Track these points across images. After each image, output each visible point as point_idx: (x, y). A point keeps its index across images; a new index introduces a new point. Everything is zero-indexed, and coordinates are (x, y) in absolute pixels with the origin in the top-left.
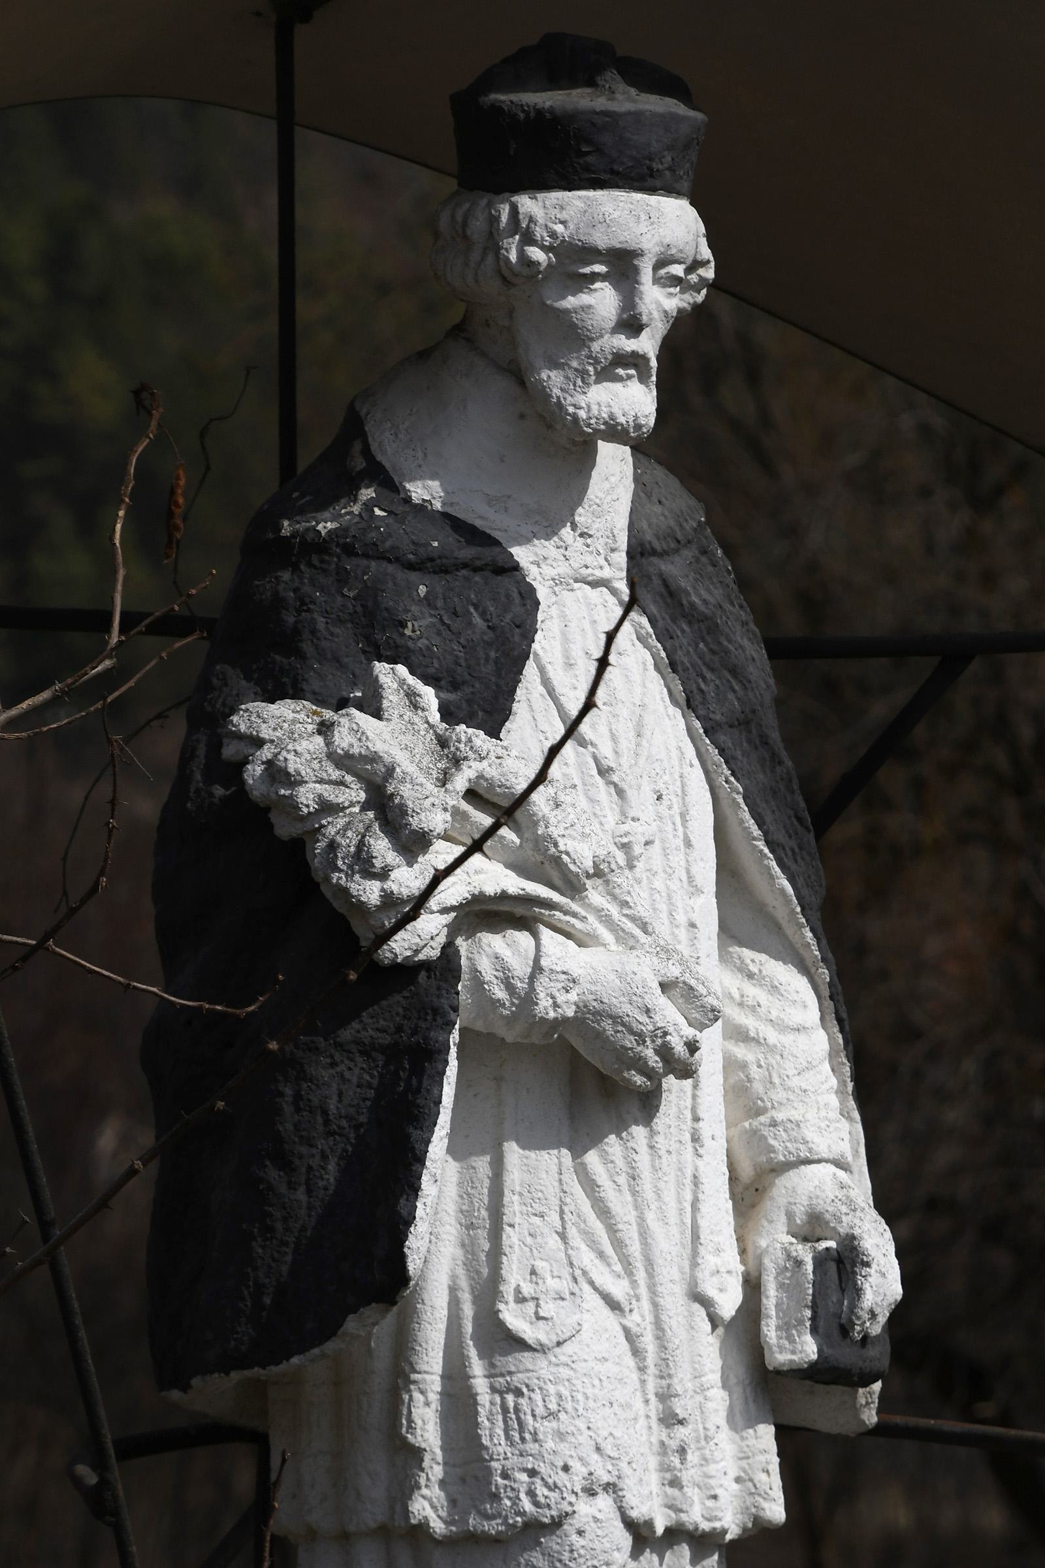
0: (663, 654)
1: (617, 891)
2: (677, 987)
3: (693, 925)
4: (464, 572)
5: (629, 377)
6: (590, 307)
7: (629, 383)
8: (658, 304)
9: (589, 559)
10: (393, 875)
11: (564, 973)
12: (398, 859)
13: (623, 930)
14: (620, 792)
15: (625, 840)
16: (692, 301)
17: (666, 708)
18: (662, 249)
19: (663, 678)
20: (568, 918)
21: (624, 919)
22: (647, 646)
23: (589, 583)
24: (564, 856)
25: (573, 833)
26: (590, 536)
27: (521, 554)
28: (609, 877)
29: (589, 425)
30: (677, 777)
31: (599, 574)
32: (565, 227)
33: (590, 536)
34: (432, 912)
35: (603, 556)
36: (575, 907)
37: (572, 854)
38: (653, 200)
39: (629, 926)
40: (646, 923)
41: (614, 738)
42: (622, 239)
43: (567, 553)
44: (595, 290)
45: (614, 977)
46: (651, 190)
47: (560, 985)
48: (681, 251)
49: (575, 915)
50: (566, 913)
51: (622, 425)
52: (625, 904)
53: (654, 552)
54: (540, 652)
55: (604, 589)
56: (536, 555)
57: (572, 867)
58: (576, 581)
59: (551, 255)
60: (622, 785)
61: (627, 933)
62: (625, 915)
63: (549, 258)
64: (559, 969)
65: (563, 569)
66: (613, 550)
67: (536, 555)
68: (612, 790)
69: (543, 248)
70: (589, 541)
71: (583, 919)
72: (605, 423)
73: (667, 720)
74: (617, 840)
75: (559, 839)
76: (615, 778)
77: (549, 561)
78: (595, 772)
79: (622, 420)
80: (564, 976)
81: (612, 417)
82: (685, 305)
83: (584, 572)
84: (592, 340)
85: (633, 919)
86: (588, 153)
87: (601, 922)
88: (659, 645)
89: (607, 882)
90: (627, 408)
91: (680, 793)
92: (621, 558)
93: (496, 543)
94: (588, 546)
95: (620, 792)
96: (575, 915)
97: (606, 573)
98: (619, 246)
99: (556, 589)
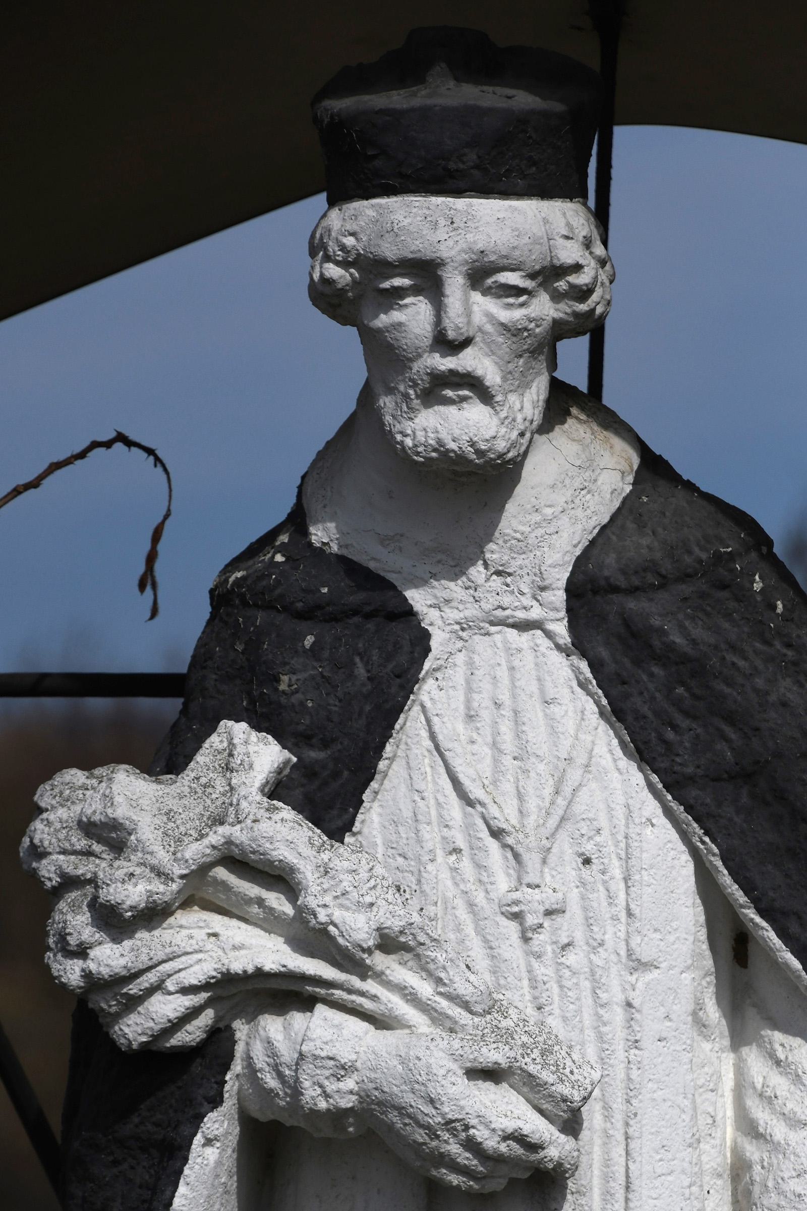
0: (604, 701)
1: (431, 966)
2: (514, 1074)
3: (629, 1005)
4: (356, 619)
5: (464, 399)
6: (400, 324)
7: (465, 405)
8: (491, 317)
9: (507, 600)
10: (92, 953)
12: (97, 935)
13: (436, 1011)
14: (517, 856)
15: (515, 909)
16: (569, 310)
17: (615, 761)
18: (474, 257)
19: (612, 727)
20: (353, 997)
21: (438, 998)
22: (590, 694)
23: (513, 626)
24: (331, 928)
25: (347, 903)
26: (510, 574)
27: (417, 598)
28: (420, 950)
29: (418, 454)
30: (620, 837)
31: (521, 615)
32: (357, 239)
33: (510, 574)
34: (170, 993)
35: (529, 595)
36: (370, 986)
37: (340, 925)
38: (460, 203)
41: (520, 797)
42: (413, 248)
43: (476, 594)
44: (406, 306)
45: (396, 1062)
46: (458, 193)
47: (327, 1073)
48: (506, 257)
49: (362, 994)
50: (350, 991)
51: (453, 451)
52: (439, 981)
53: (615, 589)
54: (428, 704)
55: (539, 632)
56: (436, 597)
57: (341, 941)
58: (492, 623)
59: (352, 270)
60: (520, 849)
61: (441, 1014)
62: (440, 994)
63: (351, 275)
64: (323, 1054)
65: (471, 611)
66: (543, 589)
67: (436, 597)
68: (509, 855)
69: (338, 263)
70: (509, 580)
71: (374, 998)
72: (435, 450)
73: (617, 774)
74: (504, 909)
75: (318, 910)
76: (510, 841)
77: (454, 604)
78: (485, 834)
79: (453, 446)
80: (332, 1063)
81: (440, 442)
82: (561, 315)
83: (499, 613)
84: (411, 360)
85: (452, 998)
86: (374, 157)
87: (407, 1001)
88: (600, 692)
89: (418, 956)
90: (457, 432)
91: (623, 856)
92: (559, 597)
93: (392, 587)
94: (508, 585)
95: (517, 856)
96: (362, 994)
97: (536, 613)
98: (411, 256)
99: (464, 634)
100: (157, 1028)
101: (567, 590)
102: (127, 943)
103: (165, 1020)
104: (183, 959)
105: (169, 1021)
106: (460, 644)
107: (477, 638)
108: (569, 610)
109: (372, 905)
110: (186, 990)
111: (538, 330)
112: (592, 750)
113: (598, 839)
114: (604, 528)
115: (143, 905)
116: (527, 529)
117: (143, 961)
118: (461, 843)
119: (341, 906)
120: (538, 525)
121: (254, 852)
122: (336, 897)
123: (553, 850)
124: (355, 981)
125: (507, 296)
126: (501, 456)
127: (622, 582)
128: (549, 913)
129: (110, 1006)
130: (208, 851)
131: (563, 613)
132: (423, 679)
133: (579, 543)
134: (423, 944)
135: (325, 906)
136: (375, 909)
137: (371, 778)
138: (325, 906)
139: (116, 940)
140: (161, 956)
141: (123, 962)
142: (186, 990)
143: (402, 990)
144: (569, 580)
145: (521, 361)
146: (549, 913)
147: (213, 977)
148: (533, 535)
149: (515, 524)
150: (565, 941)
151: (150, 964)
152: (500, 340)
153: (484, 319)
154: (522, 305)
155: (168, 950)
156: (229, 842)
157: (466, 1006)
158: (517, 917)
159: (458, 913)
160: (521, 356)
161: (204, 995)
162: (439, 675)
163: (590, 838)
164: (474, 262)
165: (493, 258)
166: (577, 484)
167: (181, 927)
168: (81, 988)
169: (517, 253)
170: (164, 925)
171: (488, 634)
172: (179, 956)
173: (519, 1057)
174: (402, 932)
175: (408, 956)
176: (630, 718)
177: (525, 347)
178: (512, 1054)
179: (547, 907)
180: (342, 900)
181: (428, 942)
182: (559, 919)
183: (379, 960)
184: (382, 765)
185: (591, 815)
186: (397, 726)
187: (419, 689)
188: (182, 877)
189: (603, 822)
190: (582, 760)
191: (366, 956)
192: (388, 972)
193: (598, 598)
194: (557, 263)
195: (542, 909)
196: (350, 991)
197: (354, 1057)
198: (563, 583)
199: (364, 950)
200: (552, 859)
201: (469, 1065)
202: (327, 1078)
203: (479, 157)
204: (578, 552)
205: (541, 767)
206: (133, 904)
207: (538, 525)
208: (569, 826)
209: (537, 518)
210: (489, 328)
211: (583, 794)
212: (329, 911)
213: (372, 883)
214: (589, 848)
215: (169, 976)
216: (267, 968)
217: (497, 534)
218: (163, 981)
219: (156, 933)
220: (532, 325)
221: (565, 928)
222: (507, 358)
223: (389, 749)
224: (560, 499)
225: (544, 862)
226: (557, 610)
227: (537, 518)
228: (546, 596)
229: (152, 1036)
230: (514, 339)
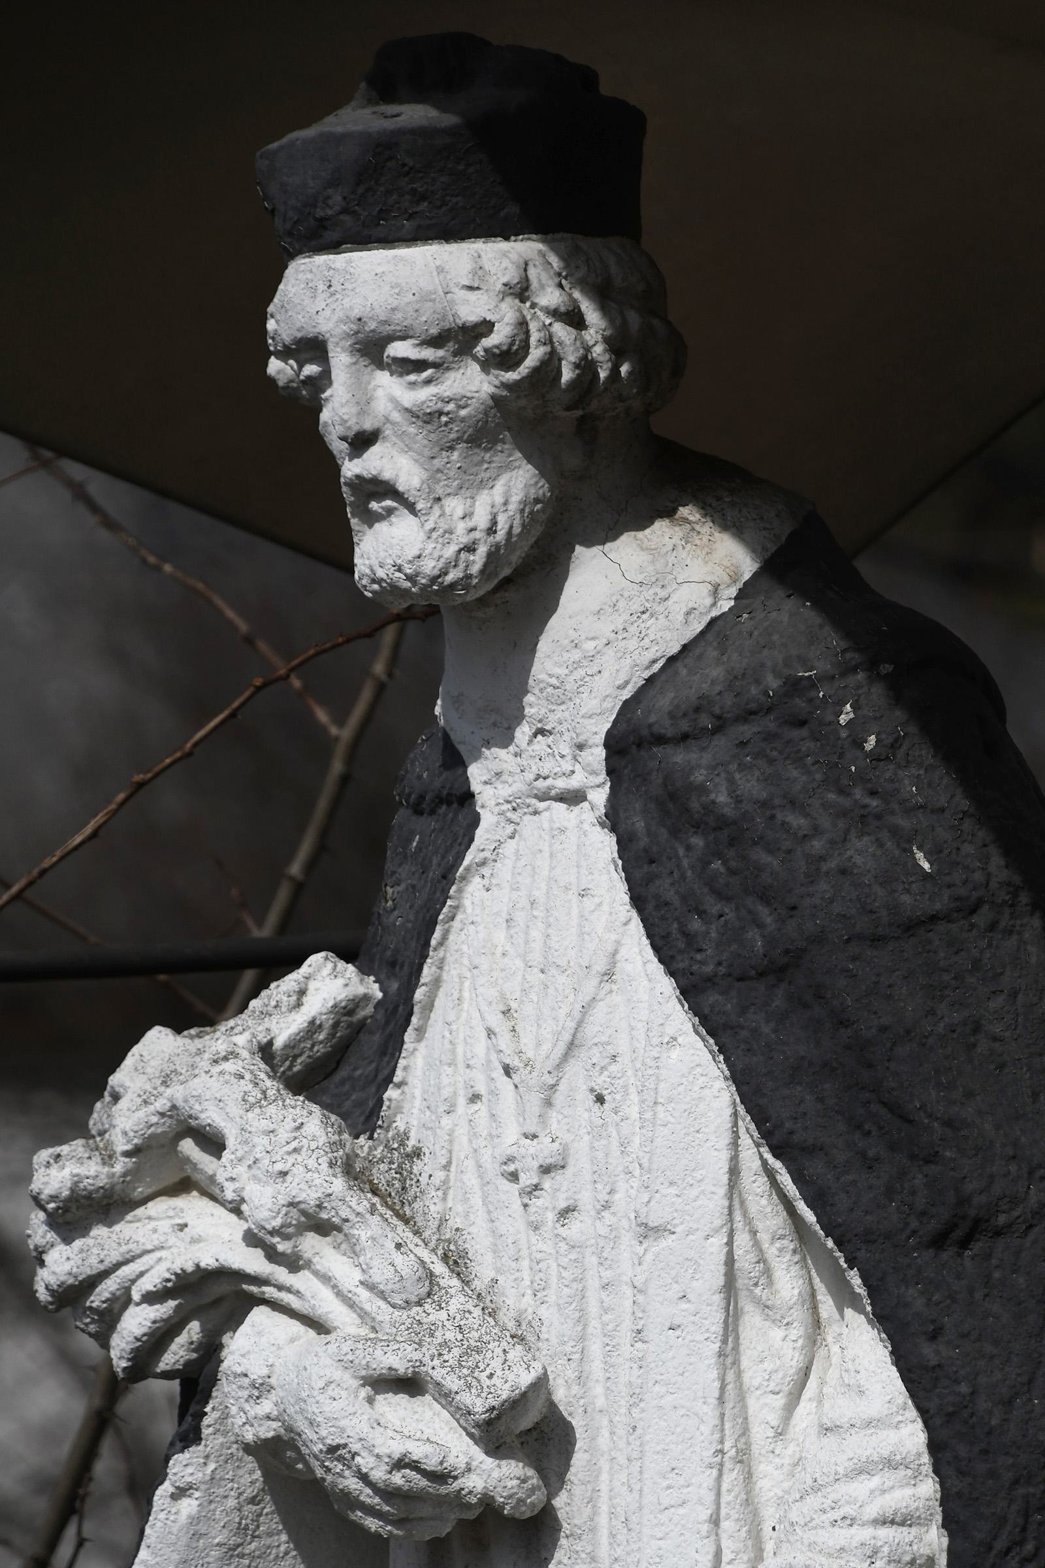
5: (390, 512)
7: (393, 519)
11: (246, 1375)
12: (49, 1235)
15: (511, 1168)
18: (354, 327)
34: (138, 1304)
35: (569, 757)
39: (364, 1295)
40: (383, 1292)
47: (245, 1393)
49: (289, 1290)
50: (280, 1288)
53: (660, 740)
58: (542, 798)
66: (581, 747)
75: (227, 1184)
77: (505, 777)
83: (541, 784)
85: (371, 1287)
92: (597, 754)
96: (289, 1290)
100: (128, 1348)
101: (607, 745)
102: (78, 1243)
103: (131, 1339)
104: (145, 1258)
105: (137, 1339)
106: (510, 829)
107: (527, 818)
108: (609, 772)
109: (284, 1174)
110: (150, 1298)
111: (463, 413)
112: (615, 953)
113: (613, 1068)
114: (672, 660)
115: (66, 1193)
116: (562, 671)
117: (92, 1266)
118: (481, 1089)
119: (255, 1177)
120: (577, 665)
121: (190, 1117)
122: (249, 1166)
123: (561, 1087)
124: (281, 1274)
125: (408, 373)
126: (434, 580)
127: (670, 732)
128: (546, 1170)
129: (86, 1324)
130: (154, 1119)
131: (603, 776)
132: (463, 878)
133: (627, 683)
134: (347, 1220)
135: (232, 1179)
136: (289, 1178)
137: (411, 1014)
138: (232, 1179)
139: (67, 1240)
140: (114, 1257)
141: (67, 1267)
142: (150, 1298)
143: (325, 1279)
144: (609, 734)
145: (455, 455)
146: (546, 1170)
147: (168, 1280)
148: (571, 679)
149: (549, 666)
150: (563, 1205)
151: (102, 1267)
152: (412, 430)
153: (390, 406)
154: (428, 382)
155: (124, 1248)
156: (174, 1107)
157: (382, 1295)
158: (514, 1177)
159: (465, 1177)
160: (451, 448)
161: (172, 1304)
162: (486, 871)
163: (603, 1068)
164: (357, 333)
165: (372, 325)
166: (636, 607)
167: (150, 1218)
168: (51, 1303)
169: (399, 316)
170: (129, 1217)
171: (536, 813)
172: (140, 1256)
173: (427, 1360)
174: (320, 1206)
175: (340, 1237)
176: (650, 907)
177: (453, 436)
178: (417, 1356)
179: (541, 1162)
180: (255, 1171)
181: (352, 1217)
182: (558, 1177)
183: (310, 1244)
184: (419, 994)
185: (604, 1039)
186: (433, 942)
187: (460, 891)
188: (127, 1154)
189: (622, 1045)
190: (600, 966)
191: (276, 1240)
192: (315, 1260)
193: (643, 753)
194: (460, 323)
195: (535, 1164)
196: (280, 1288)
197: (265, 1372)
198: (600, 738)
199: (273, 1233)
200: (559, 1098)
201: (364, 1373)
202: (247, 1401)
203: (345, 198)
204: (626, 694)
205: (562, 979)
206: (53, 1193)
207: (577, 665)
208: (583, 1054)
209: (576, 655)
210: (396, 416)
211: (599, 1013)
212: (237, 1185)
213: (294, 1144)
214: (600, 1082)
215: (133, 1281)
216: (203, 1265)
217: (531, 682)
218: (128, 1290)
219: (117, 1228)
220: (451, 407)
221: (564, 1189)
222: (427, 452)
223: (427, 973)
224: (605, 629)
225: (548, 1103)
226: (594, 773)
227: (576, 655)
228: (586, 756)
229: (129, 1360)
230: (429, 427)
